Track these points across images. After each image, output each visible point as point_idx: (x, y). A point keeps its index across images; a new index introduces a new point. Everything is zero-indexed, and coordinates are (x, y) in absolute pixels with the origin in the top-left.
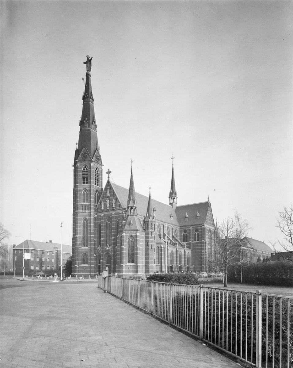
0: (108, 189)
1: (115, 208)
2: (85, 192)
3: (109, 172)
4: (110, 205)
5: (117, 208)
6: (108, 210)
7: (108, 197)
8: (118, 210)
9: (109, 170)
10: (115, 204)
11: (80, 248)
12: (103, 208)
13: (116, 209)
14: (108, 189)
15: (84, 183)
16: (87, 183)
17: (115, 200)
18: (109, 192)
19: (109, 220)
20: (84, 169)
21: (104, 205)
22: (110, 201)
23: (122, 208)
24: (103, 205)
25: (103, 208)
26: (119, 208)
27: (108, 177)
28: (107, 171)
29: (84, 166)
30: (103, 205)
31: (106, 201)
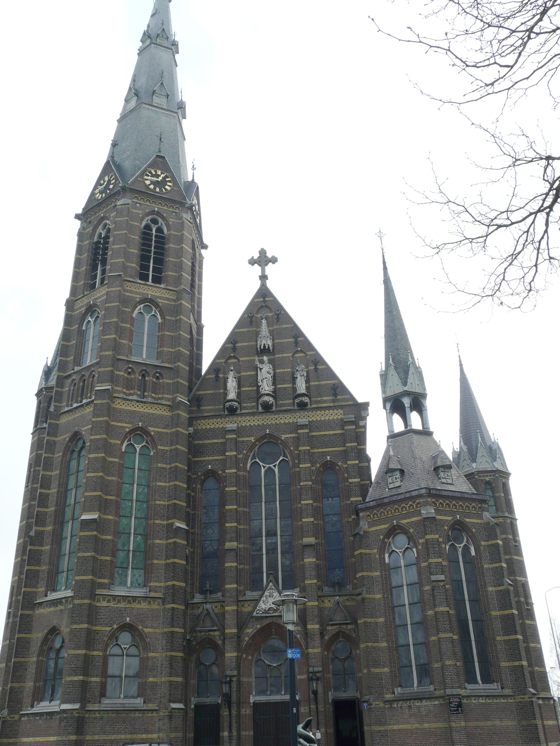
0: (264, 321)
1: (306, 400)
2: (147, 317)
3: (263, 260)
4: (274, 384)
5: (320, 402)
6: (267, 407)
7: (265, 351)
8: (328, 408)
9: (263, 252)
10: (307, 381)
11: (105, 592)
12: (232, 395)
13: (314, 406)
14: (264, 321)
15: (144, 277)
16: (157, 280)
17: (307, 366)
18: (271, 333)
19: (269, 457)
20: (147, 227)
21: (239, 386)
22: (274, 370)
23: (350, 403)
24: (232, 384)
25: (232, 395)
26: (333, 401)
27: (263, 278)
28: (256, 256)
29: (150, 217)
30: (232, 384)
31: (256, 369)
